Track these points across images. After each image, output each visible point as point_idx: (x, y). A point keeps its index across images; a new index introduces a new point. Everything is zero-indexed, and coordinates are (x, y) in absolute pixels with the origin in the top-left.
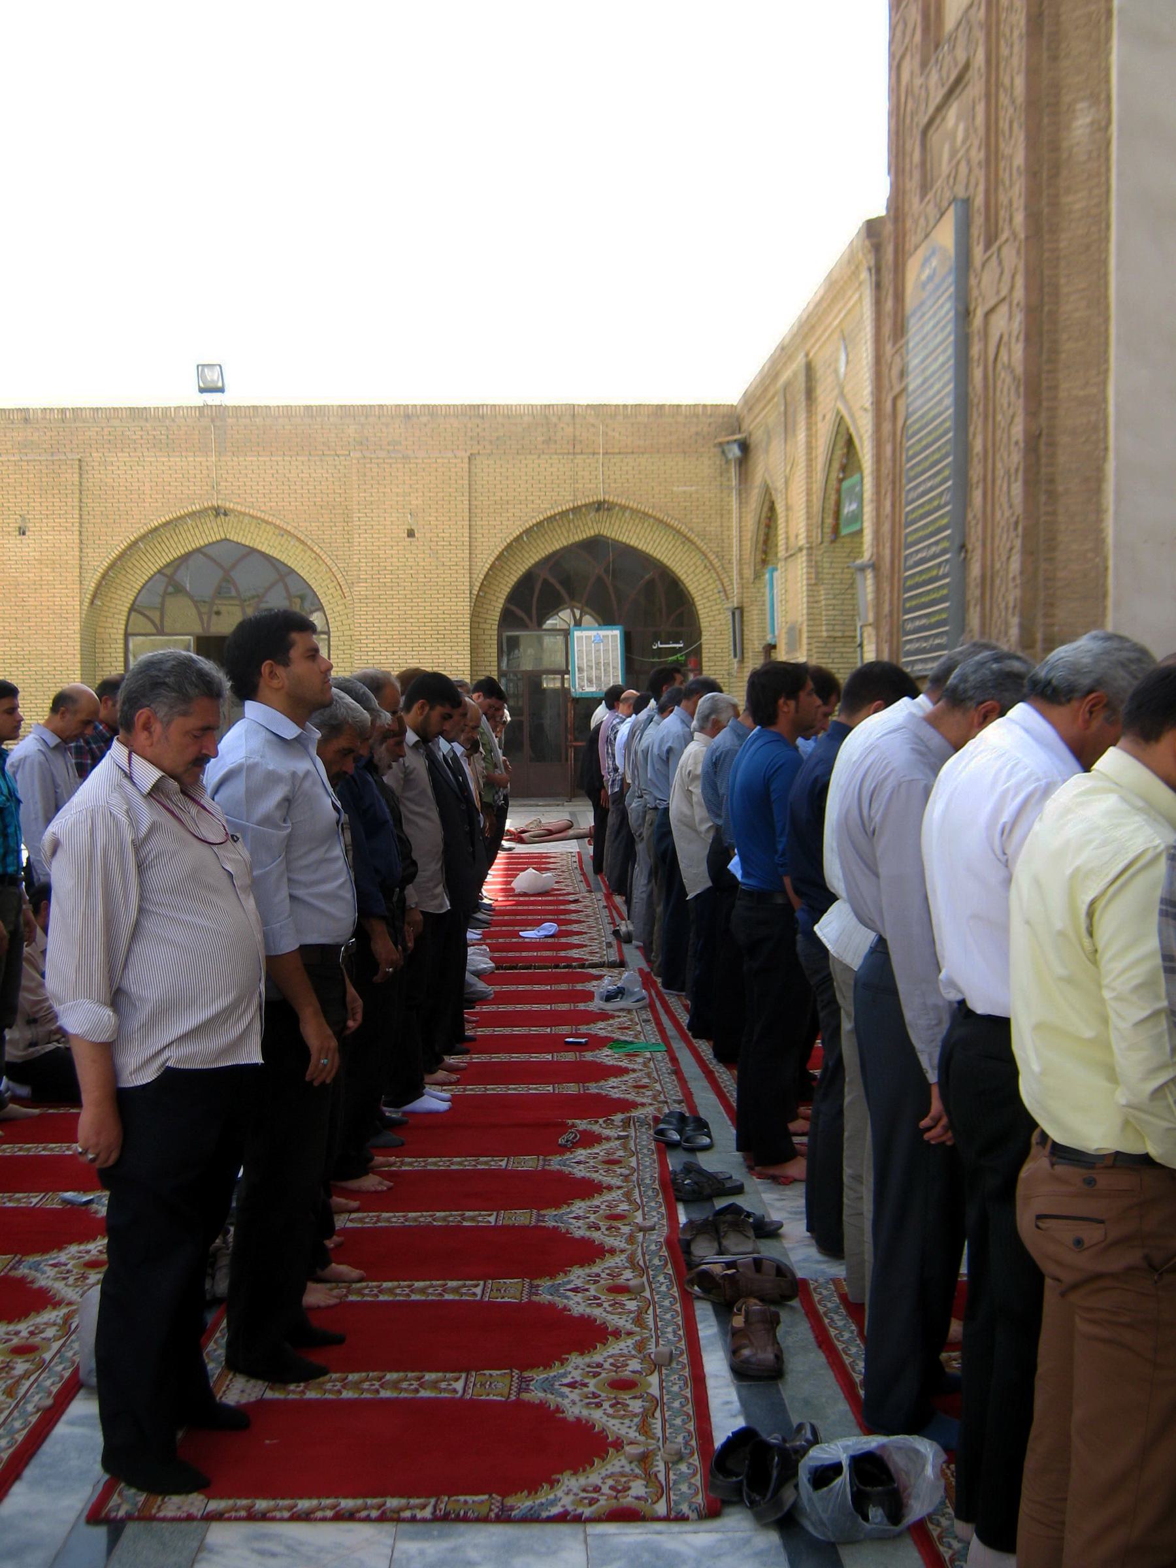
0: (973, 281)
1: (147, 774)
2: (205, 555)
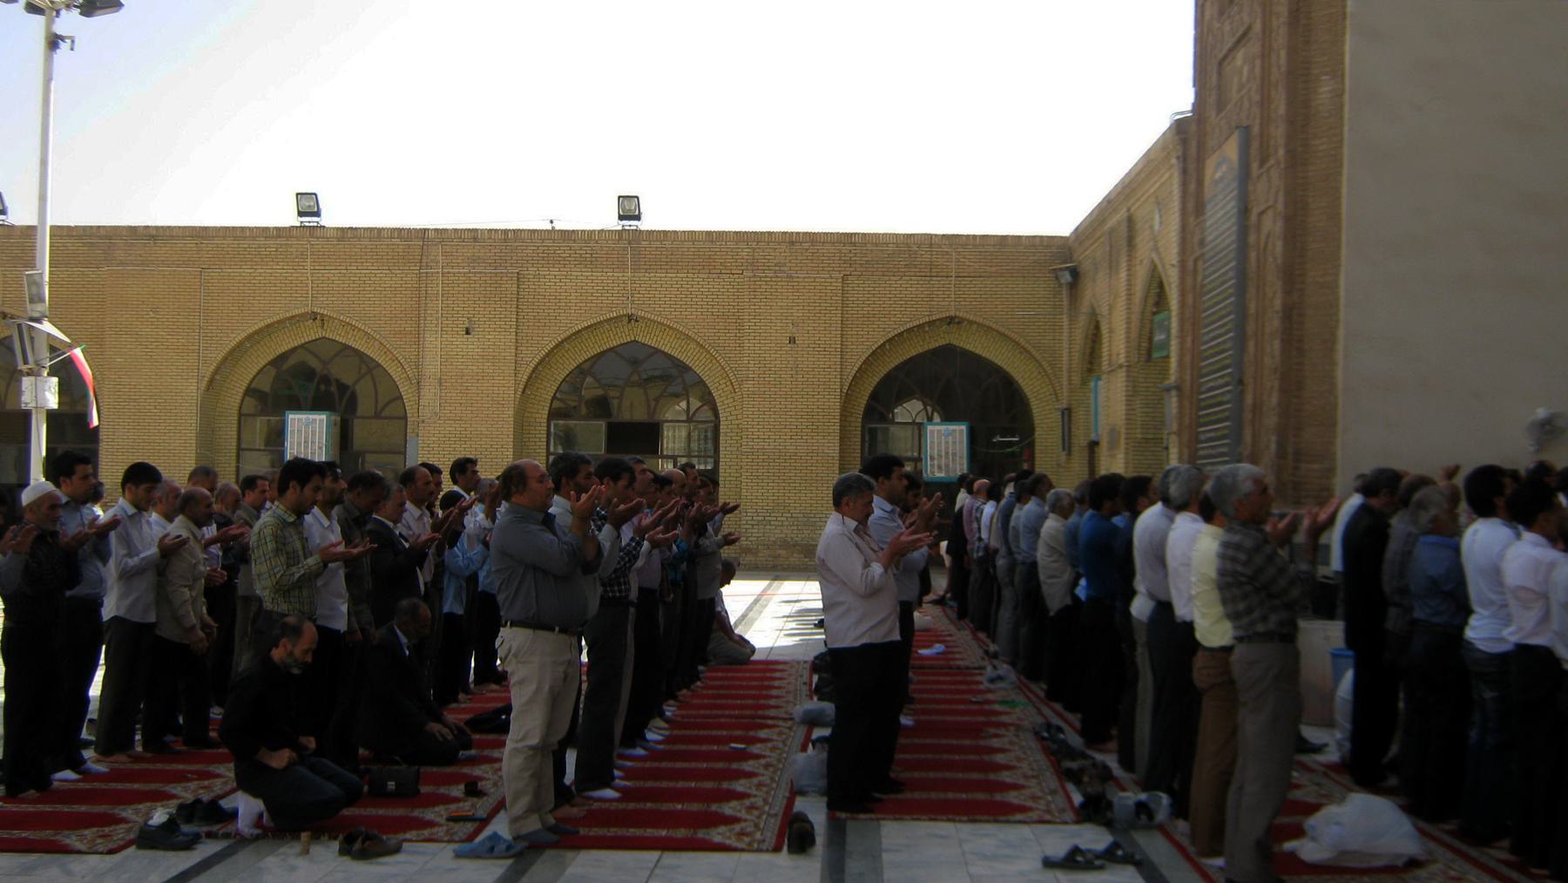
0: (1251, 188)
1: (853, 524)
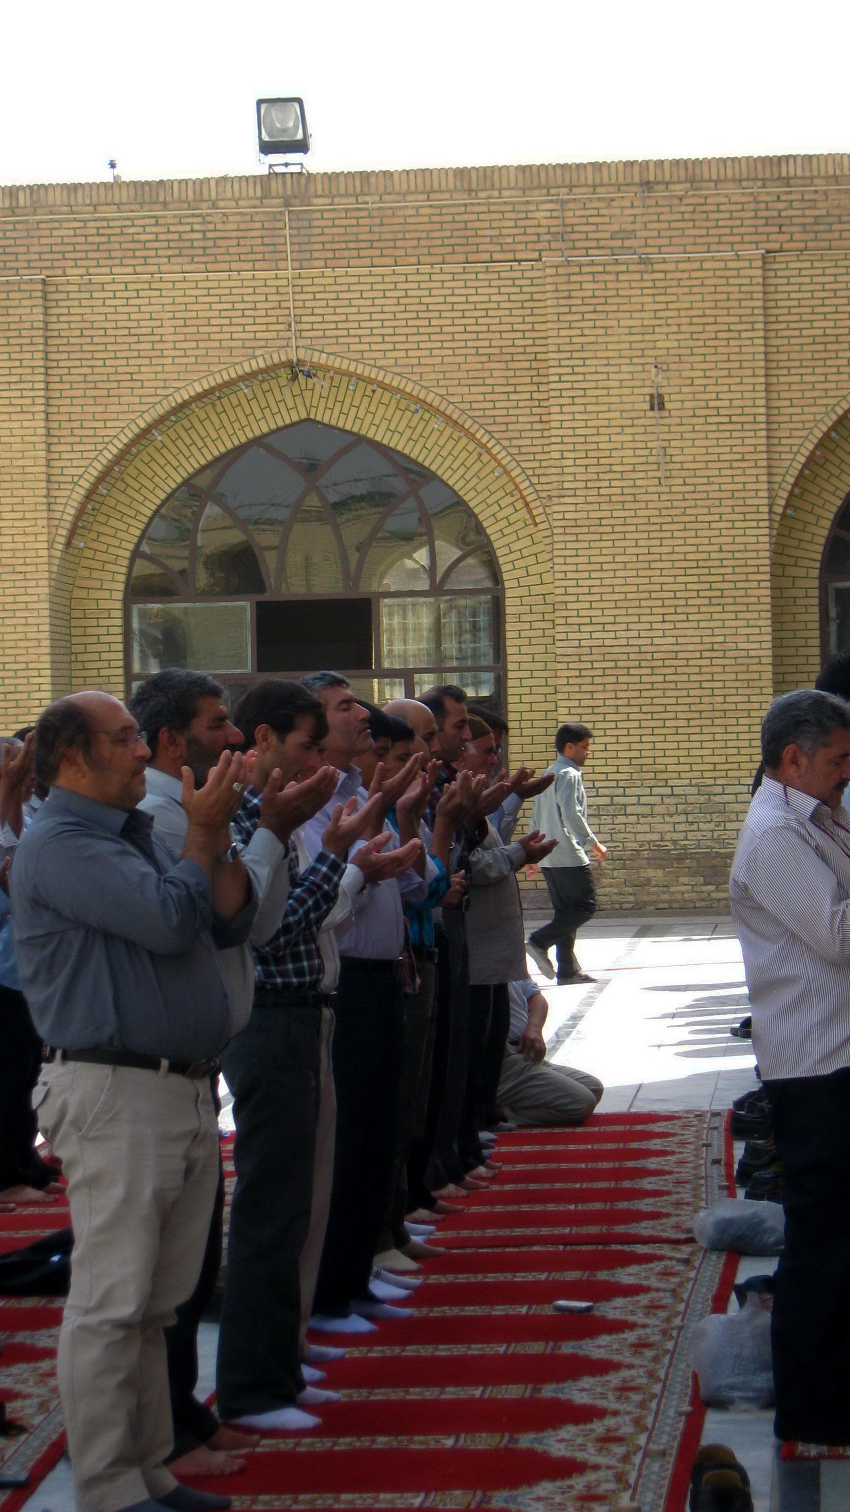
1: (807, 803)
2: (270, 449)
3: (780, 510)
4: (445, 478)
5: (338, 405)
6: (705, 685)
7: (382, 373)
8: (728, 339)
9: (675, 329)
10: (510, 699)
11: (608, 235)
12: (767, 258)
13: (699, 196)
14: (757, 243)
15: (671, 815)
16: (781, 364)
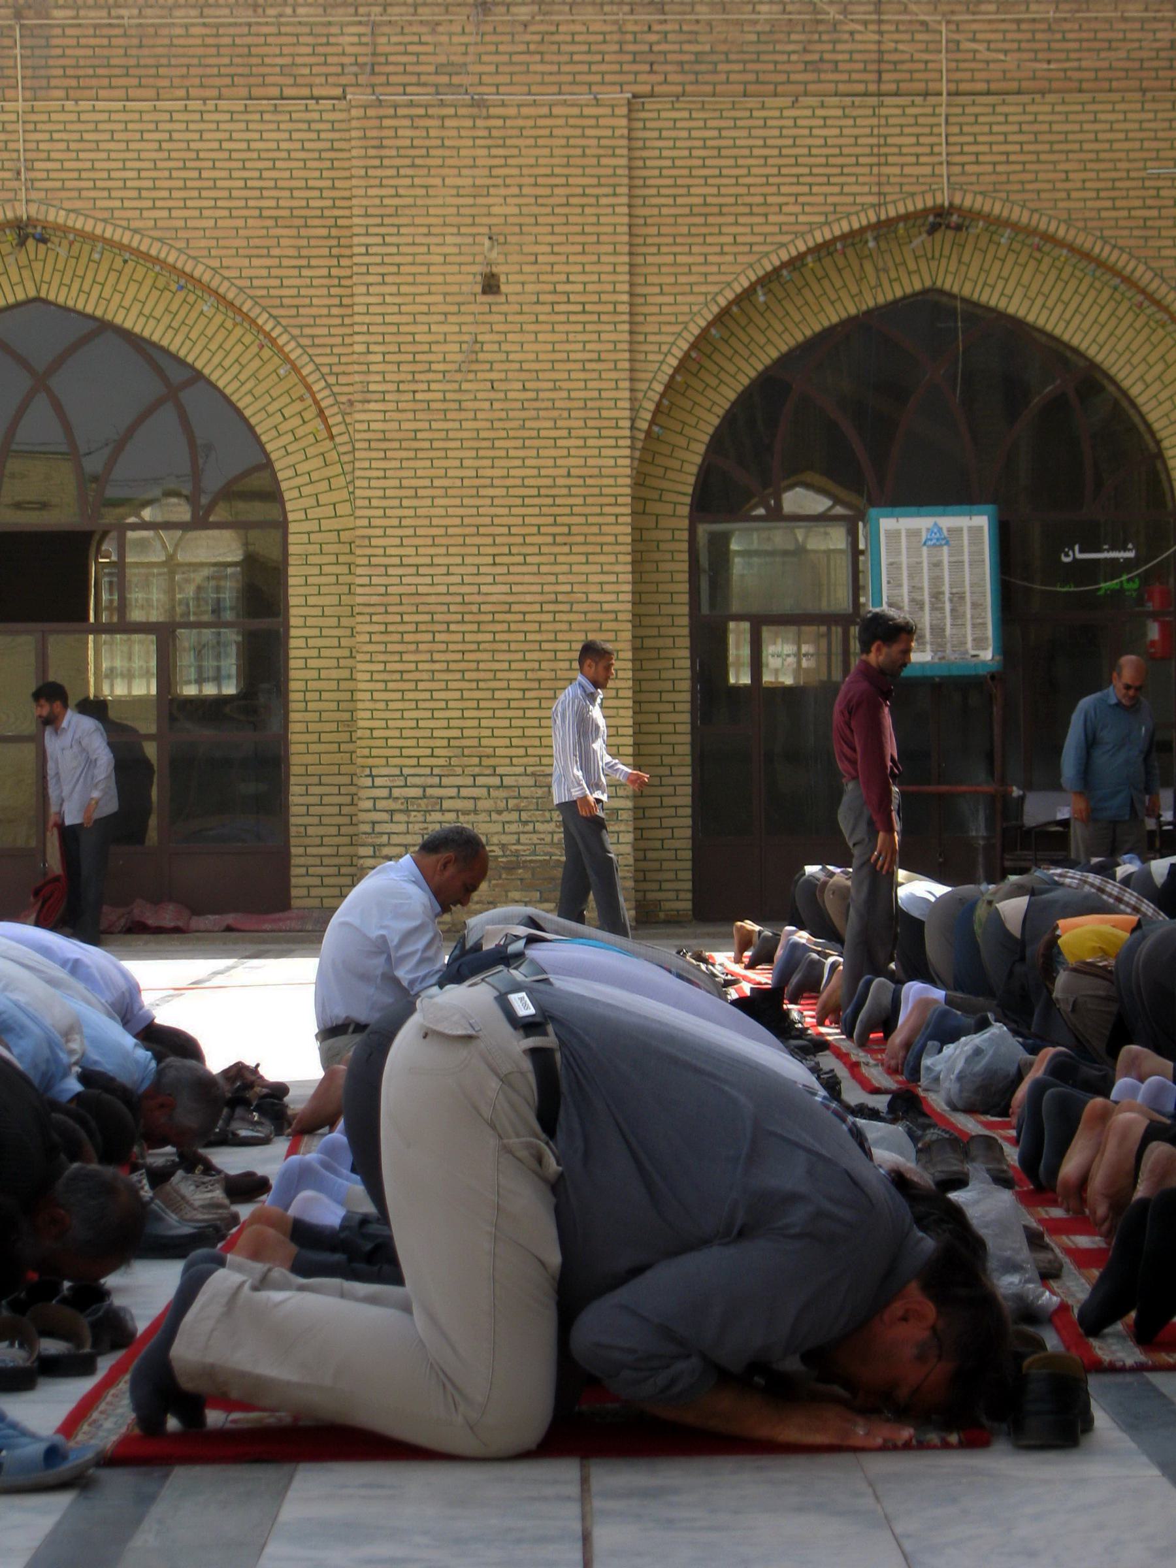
3: (644, 426)
4: (213, 378)
5: (77, 282)
6: (545, 646)
7: (137, 237)
8: (583, 206)
9: (516, 191)
10: (293, 663)
11: (432, 69)
12: (635, 103)
13: (551, 23)
14: (621, 85)
15: (499, 812)
16: (649, 240)
